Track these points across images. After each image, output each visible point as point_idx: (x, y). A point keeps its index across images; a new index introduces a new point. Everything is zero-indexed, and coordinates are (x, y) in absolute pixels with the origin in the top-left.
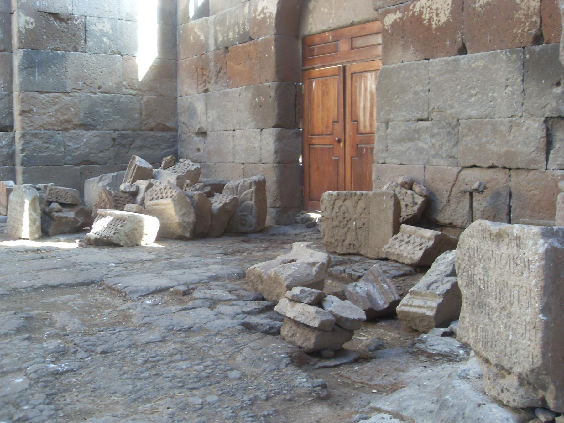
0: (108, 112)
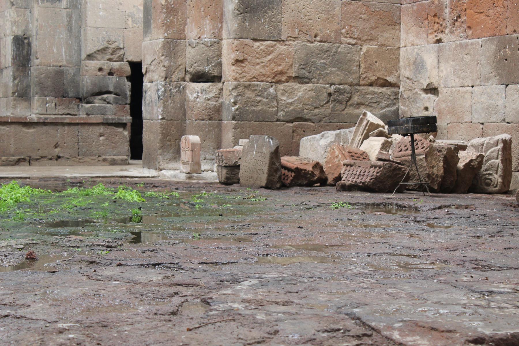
0: (324, 63)
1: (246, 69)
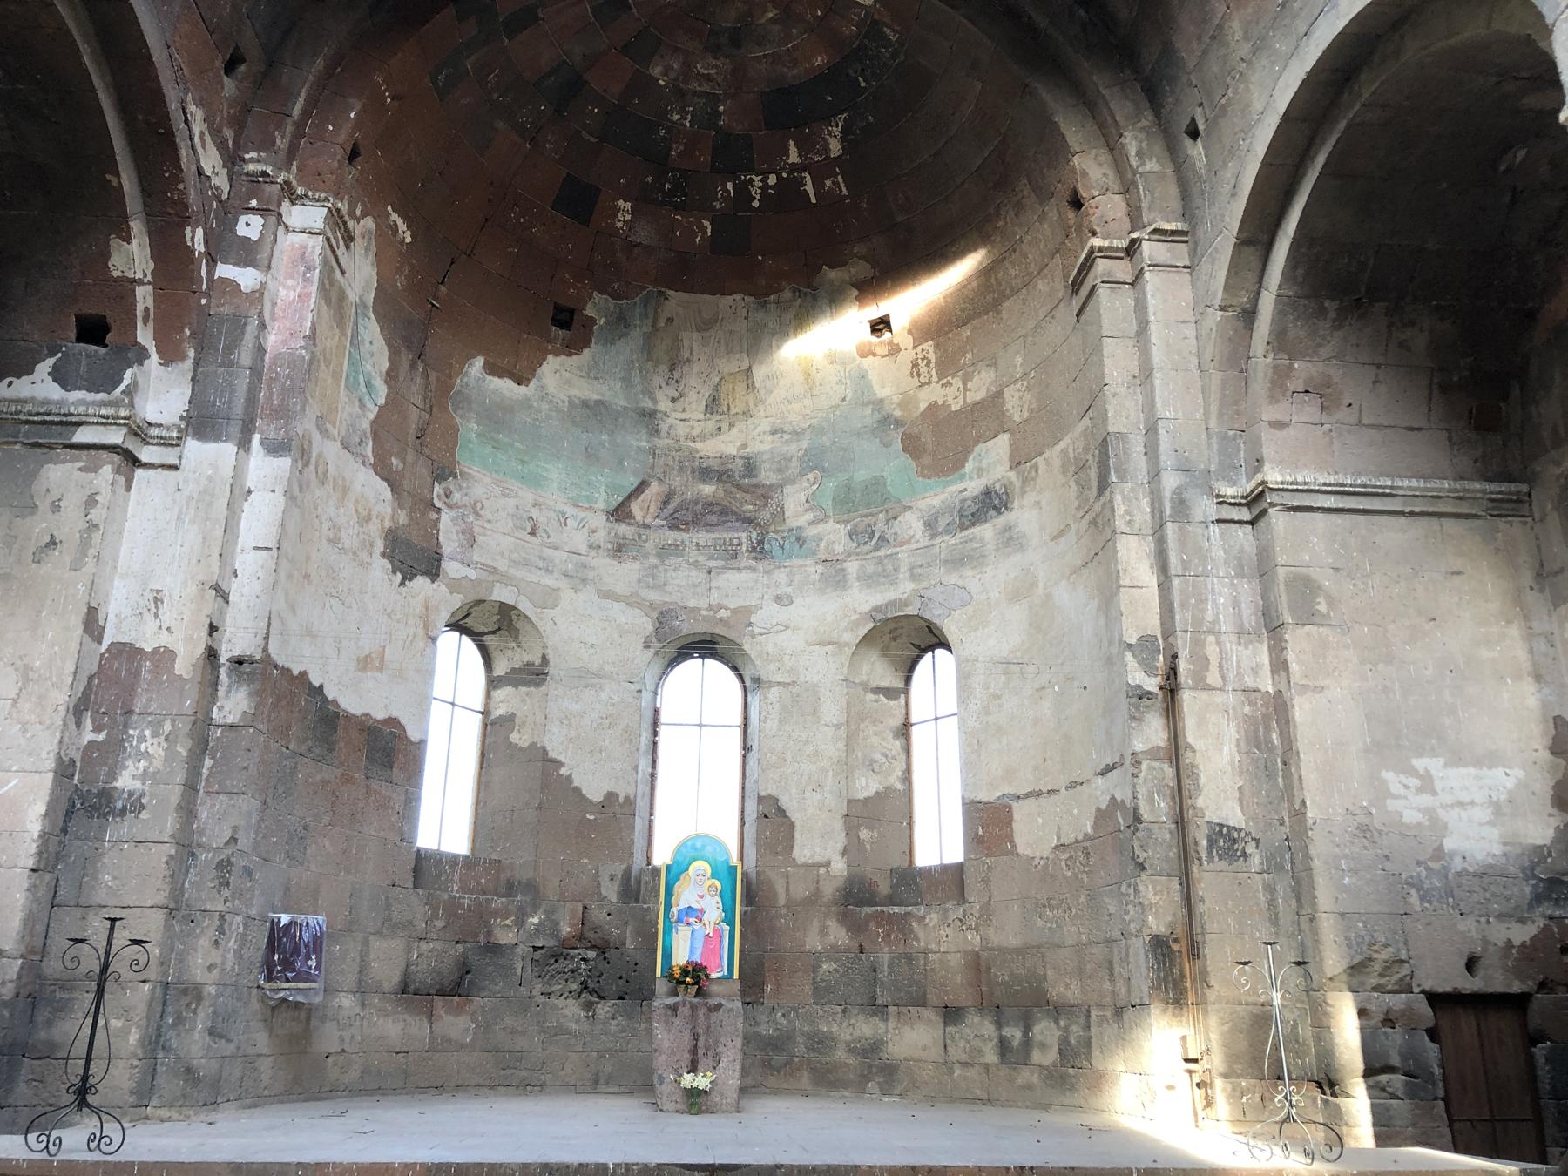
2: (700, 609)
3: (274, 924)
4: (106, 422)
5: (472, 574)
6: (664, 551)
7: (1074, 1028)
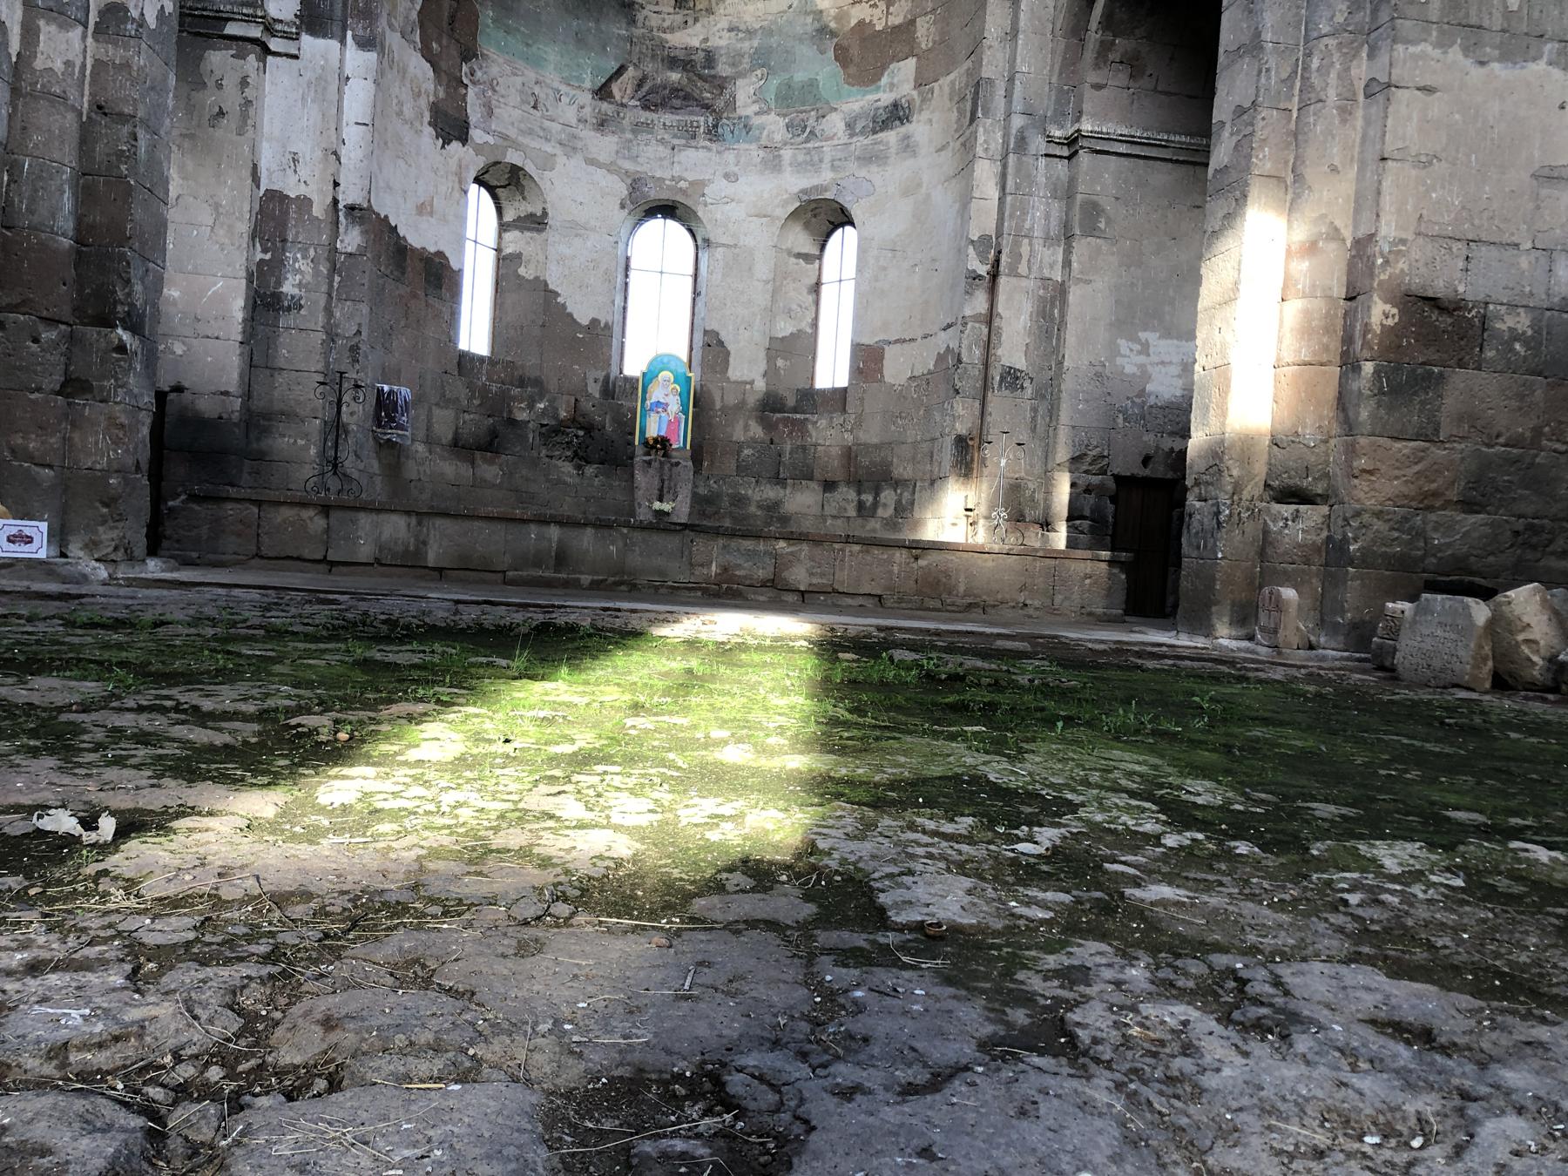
0: (1508, 481)
1: (1377, 485)
2: (664, 179)
3: (380, 391)
4: (249, 19)
5: (491, 140)
6: (638, 127)
7: (906, 494)
